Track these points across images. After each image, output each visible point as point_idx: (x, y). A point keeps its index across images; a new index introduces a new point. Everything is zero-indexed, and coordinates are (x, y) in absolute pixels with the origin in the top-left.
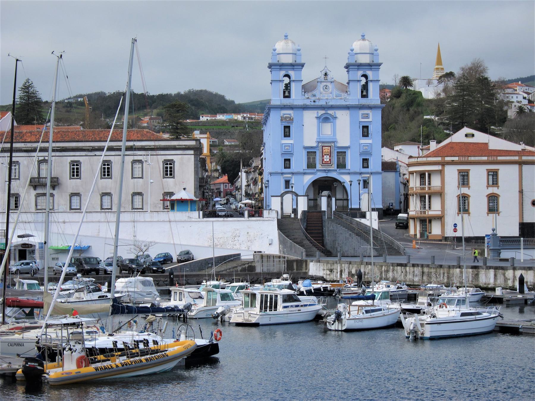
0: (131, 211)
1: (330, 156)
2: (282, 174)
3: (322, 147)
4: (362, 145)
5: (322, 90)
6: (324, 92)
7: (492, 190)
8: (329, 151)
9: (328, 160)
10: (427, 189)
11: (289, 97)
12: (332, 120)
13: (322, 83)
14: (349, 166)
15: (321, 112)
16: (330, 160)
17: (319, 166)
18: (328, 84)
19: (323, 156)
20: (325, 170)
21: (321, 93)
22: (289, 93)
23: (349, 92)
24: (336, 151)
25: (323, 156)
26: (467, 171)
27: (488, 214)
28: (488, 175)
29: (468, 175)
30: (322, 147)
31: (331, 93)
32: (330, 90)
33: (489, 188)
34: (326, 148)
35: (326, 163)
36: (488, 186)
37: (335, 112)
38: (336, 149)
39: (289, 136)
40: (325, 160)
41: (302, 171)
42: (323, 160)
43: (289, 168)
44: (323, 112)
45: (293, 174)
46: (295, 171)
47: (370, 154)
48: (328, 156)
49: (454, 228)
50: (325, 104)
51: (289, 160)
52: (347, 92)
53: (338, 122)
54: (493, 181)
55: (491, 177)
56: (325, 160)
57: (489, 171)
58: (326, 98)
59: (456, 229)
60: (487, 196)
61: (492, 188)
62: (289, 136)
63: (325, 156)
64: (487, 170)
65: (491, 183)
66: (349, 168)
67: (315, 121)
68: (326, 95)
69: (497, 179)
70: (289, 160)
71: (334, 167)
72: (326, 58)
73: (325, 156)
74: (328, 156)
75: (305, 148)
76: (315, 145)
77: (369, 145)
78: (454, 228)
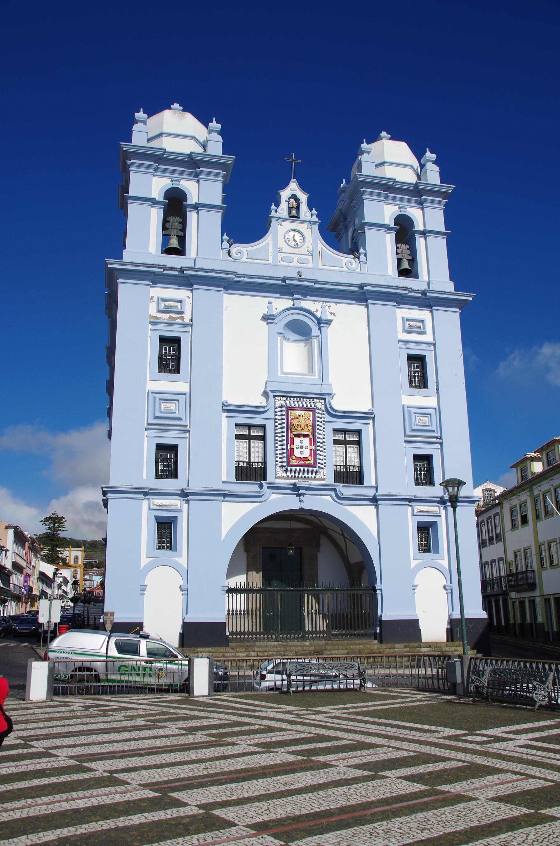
1: (313, 442)
2: (146, 493)
3: (288, 409)
4: (413, 410)
6: (286, 249)
8: (310, 423)
9: (307, 453)
11: (180, 251)
13: (283, 223)
16: (313, 453)
18: (302, 227)
19: (290, 441)
20: (295, 489)
21: (280, 251)
22: (182, 240)
23: (362, 257)
24: (329, 428)
30: (288, 409)
31: (310, 254)
34: (298, 413)
35: (302, 463)
39: (177, 370)
40: (297, 453)
41: (218, 487)
42: (291, 452)
43: (175, 475)
45: (184, 495)
46: (195, 485)
47: (439, 441)
48: (306, 441)
50: (297, 276)
51: (174, 448)
58: (295, 263)
62: (177, 370)
63: (297, 440)
66: (373, 484)
68: (296, 257)
70: (174, 448)
75: (229, 409)
76: (260, 401)
77: (432, 412)
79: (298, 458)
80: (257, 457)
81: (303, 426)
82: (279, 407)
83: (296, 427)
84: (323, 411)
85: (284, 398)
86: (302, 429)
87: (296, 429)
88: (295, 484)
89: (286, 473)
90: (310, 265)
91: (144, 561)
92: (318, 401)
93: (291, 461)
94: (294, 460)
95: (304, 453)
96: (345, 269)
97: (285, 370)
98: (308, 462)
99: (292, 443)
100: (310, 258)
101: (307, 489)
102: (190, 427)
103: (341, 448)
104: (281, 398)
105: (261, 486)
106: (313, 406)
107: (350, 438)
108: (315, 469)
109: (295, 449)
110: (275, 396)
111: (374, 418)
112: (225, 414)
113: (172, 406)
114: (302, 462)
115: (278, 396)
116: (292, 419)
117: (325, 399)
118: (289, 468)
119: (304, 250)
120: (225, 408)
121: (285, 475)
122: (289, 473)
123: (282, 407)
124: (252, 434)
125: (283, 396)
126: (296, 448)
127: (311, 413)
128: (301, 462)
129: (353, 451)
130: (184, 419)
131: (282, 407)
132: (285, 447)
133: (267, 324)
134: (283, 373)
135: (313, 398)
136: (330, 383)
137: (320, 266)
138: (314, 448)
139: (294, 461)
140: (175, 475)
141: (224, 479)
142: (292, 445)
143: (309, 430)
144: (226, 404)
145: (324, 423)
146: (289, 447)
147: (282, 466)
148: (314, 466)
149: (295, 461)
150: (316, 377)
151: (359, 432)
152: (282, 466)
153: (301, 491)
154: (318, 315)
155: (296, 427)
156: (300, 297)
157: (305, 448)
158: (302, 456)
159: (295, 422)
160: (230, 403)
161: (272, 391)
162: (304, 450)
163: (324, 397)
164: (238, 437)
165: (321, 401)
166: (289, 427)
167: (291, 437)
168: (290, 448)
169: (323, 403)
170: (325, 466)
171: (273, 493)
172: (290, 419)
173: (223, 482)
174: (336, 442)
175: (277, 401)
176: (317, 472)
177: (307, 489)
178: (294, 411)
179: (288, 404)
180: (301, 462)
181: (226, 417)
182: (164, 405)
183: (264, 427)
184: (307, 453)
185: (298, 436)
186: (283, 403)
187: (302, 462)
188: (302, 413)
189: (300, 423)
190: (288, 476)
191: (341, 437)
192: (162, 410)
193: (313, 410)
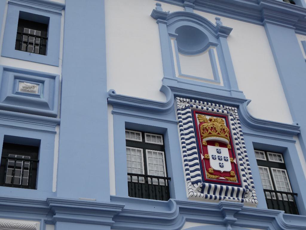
1: (232, 153)
9: (228, 167)
19: (202, 149)
24: (249, 141)
25: (202, 149)
30: (195, 112)
34: (208, 117)
38: (246, 130)
40: (214, 165)
42: (205, 164)
43: (32, 184)
44: (180, 9)
48: (225, 152)
56: (214, 165)
63: (212, 150)
74: (225, 152)
81: (219, 130)
82: (183, 110)
83: (209, 131)
84: (238, 120)
85: (188, 100)
86: (219, 134)
87: (210, 133)
88: (219, 207)
89: (202, 192)
92: (230, 108)
93: (208, 176)
94: (211, 174)
95: (224, 165)
97: (183, 73)
98: (232, 179)
99: (207, 153)
101: (236, 214)
102: (60, 118)
104: (185, 100)
105: (169, 206)
106: (225, 112)
107: (273, 159)
108: (241, 189)
109: (211, 160)
110: (175, 96)
111: (298, 135)
112: (111, 109)
113: (36, 89)
114: (223, 178)
115: (180, 96)
116: (201, 123)
117: (238, 107)
118: (207, 184)
120: (109, 99)
121: (202, 195)
122: (206, 192)
123: (186, 108)
124: (146, 141)
125: (186, 97)
126: (213, 158)
127: (224, 119)
128: (221, 178)
130: (50, 105)
131: (186, 108)
132: (196, 156)
133: (158, 23)
134: (181, 75)
135: (224, 104)
136: (240, 90)
138: (235, 161)
139: (211, 176)
140: (32, 184)
141: (113, 193)
142: (206, 155)
143: (226, 136)
144: (113, 94)
145: (242, 133)
146: (202, 157)
147: (197, 182)
149: (213, 176)
151: (282, 152)
152: (197, 182)
153: (229, 217)
154: (215, 25)
155: (209, 131)
156: (192, 4)
157: (225, 160)
158: (222, 170)
160: (118, 92)
161: (173, 89)
162: (223, 161)
164: (130, 143)
165: (233, 108)
166: (198, 132)
167: (204, 144)
168: (204, 159)
169: (236, 111)
170: (253, 187)
171: (188, 220)
172: (198, 123)
173: (112, 198)
175: (179, 101)
176: (244, 193)
177: (236, 214)
178: (203, 115)
179: (194, 106)
180: (221, 178)
181: (113, 113)
182: (22, 86)
183: (162, 133)
184: (228, 167)
185: (212, 143)
186: (187, 105)
187: (223, 178)
189: (215, 126)
190: (206, 197)
192: (19, 91)
193: (225, 117)
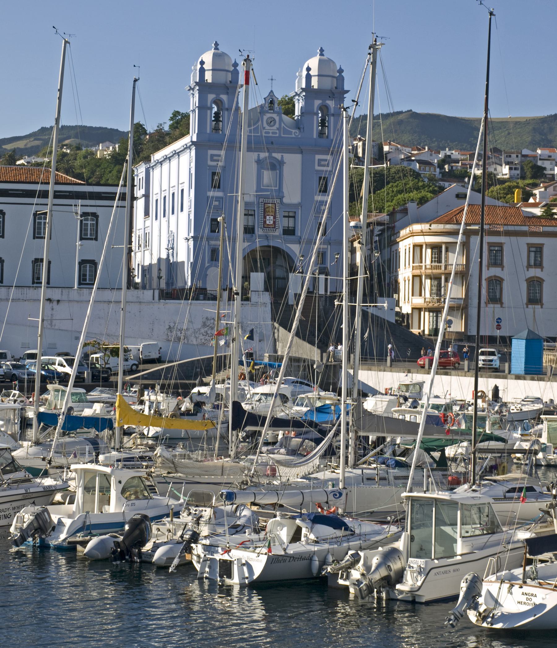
0: (32, 285)
1: (275, 218)
5: (265, 125)
6: (267, 127)
7: (534, 272)
9: (272, 222)
10: (443, 268)
12: (278, 167)
14: (298, 233)
15: (264, 155)
16: (274, 222)
17: (259, 231)
19: (265, 217)
21: (264, 128)
26: (501, 245)
27: (527, 305)
28: (529, 252)
29: (502, 251)
32: (277, 125)
33: (530, 269)
36: (529, 266)
37: (282, 156)
40: (268, 222)
42: (265, 222)
49: (497, 324)
52: (299, 128)
53: (286, 169)
54: (535, 260)
55: (532, 254)
57: (530, 246)
58: (271, 135)
59: (500, 325)
60: (526, 280)
61: (534, 269)
64: (528, 244)
65: (532, 262)
67: (254, 166)
69: (541, 257)
71: (279, 232)
72: (272, 80)
73: (268, 217)
74: (272, 217)
78: (497, 324)
79: (268, 225)
80: (250, 224)
90: (277, 135)
91: (207, 265)
93: (265, 226)
96: (293, 136)
100: (277, 131)
103: (287, 219)
107: (291, 214)
119: (275, 128)
129: (291, 220)
137: (282, 135)
148: (275, 228)
150: (277, 188)
159: (267, 210)
163: (281, 198)
174: (284, 217)
185: (268, 215)
188: (270, 205)
191: (286, 214)
